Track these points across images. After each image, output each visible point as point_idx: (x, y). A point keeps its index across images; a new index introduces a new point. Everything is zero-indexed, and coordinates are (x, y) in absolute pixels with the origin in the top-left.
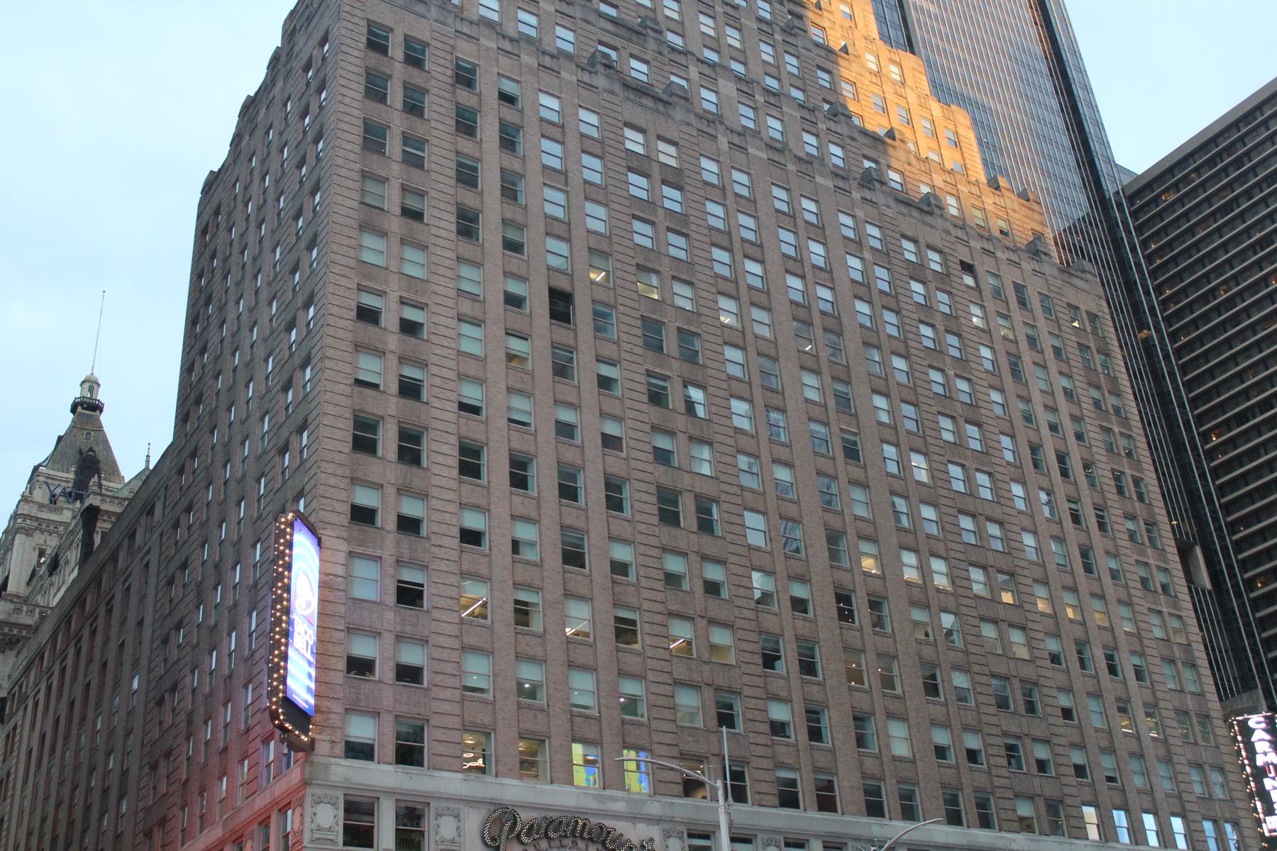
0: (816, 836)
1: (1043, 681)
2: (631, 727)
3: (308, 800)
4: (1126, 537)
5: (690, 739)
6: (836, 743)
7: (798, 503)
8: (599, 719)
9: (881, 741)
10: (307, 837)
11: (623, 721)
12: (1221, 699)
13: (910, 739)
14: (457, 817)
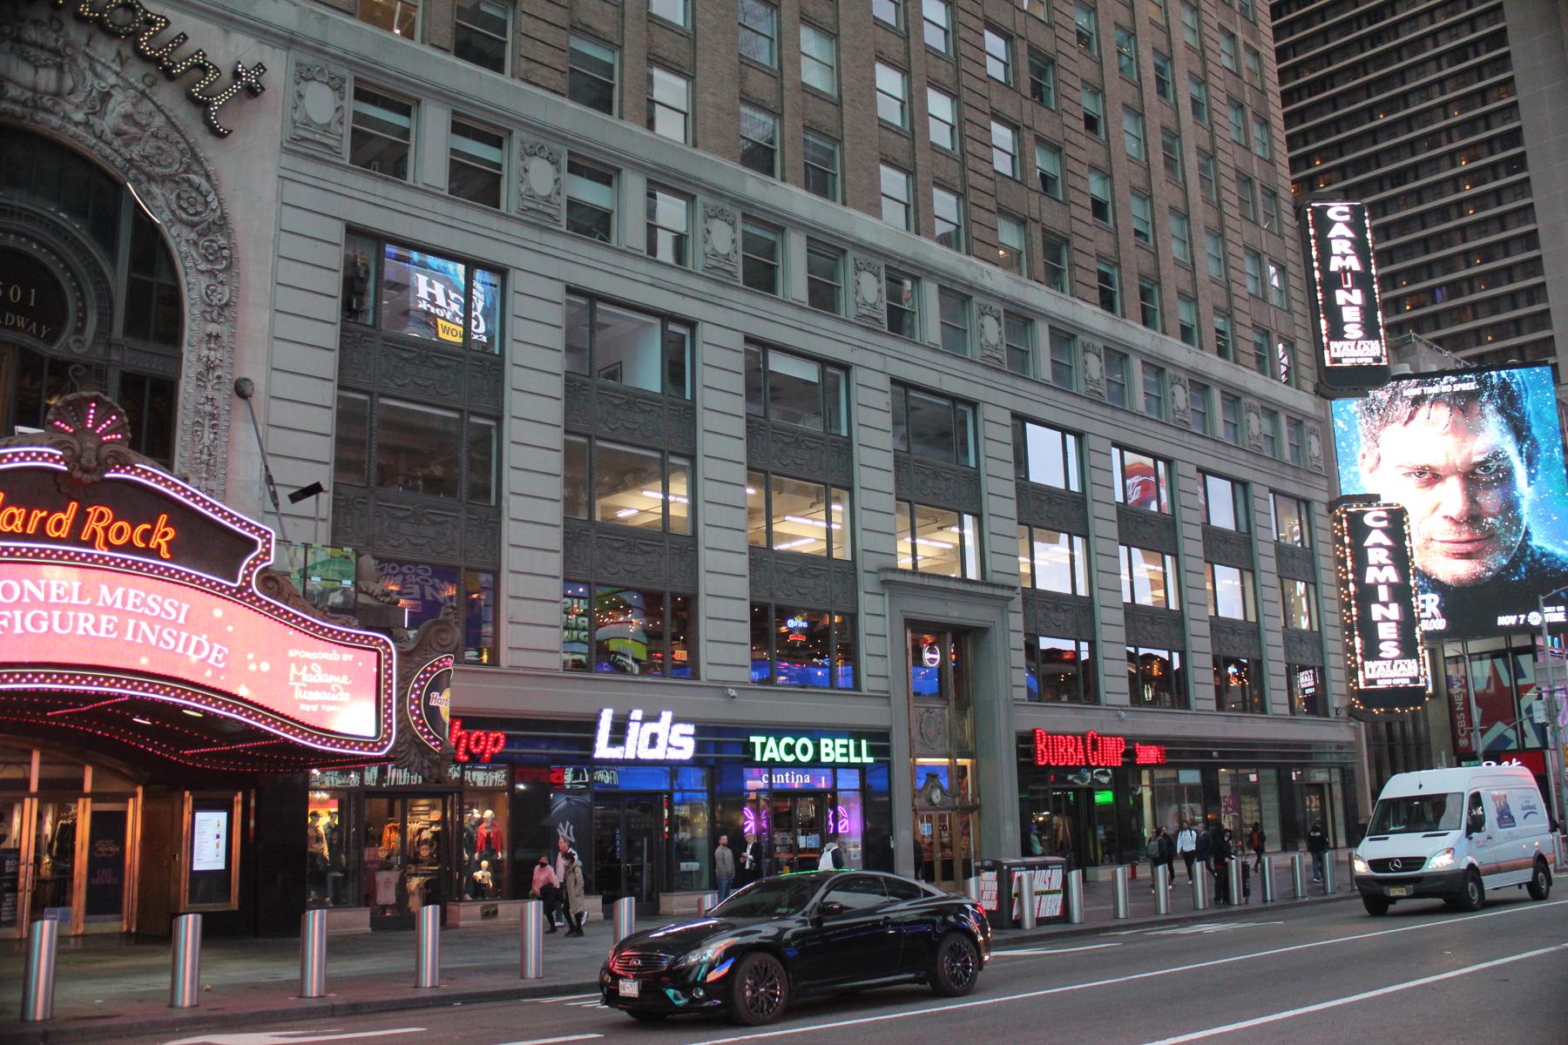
0: (638, 166)
1: (1061, 60)
6: (699, 26)
9: (784, 52)
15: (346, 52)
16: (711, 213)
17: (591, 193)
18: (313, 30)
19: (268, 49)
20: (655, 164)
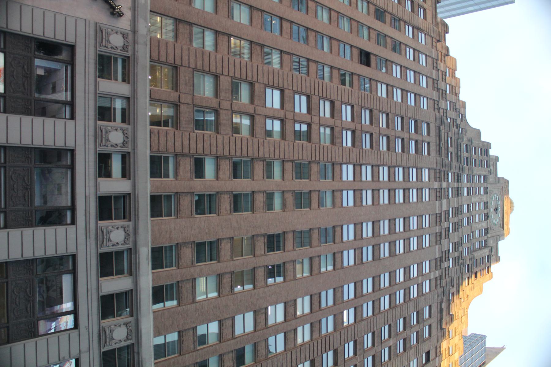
0: (134, 186)
2: (188, 31)
5: (187, 78)
13: (207, 300)
15: (137, 52)
16: (126, 229)
17: (116, 165)
18: (141, 40)
19: (129, 23)
20: (138, 194)
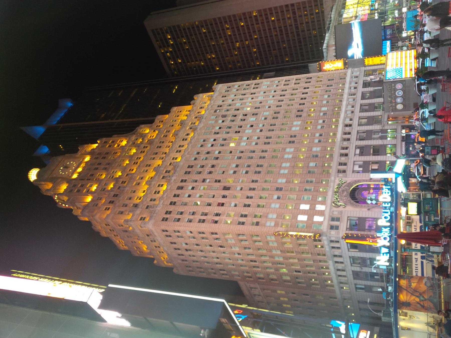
3: (330, 236)
4: (277, 87)
7: (270, 148)
8: (314, 186)
10: (337, 236)
11: (315, 182)
12: (309, 73)
14: (333, 211)
